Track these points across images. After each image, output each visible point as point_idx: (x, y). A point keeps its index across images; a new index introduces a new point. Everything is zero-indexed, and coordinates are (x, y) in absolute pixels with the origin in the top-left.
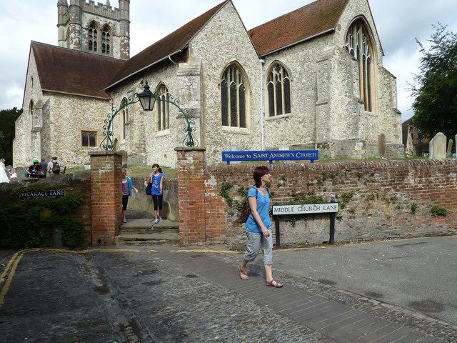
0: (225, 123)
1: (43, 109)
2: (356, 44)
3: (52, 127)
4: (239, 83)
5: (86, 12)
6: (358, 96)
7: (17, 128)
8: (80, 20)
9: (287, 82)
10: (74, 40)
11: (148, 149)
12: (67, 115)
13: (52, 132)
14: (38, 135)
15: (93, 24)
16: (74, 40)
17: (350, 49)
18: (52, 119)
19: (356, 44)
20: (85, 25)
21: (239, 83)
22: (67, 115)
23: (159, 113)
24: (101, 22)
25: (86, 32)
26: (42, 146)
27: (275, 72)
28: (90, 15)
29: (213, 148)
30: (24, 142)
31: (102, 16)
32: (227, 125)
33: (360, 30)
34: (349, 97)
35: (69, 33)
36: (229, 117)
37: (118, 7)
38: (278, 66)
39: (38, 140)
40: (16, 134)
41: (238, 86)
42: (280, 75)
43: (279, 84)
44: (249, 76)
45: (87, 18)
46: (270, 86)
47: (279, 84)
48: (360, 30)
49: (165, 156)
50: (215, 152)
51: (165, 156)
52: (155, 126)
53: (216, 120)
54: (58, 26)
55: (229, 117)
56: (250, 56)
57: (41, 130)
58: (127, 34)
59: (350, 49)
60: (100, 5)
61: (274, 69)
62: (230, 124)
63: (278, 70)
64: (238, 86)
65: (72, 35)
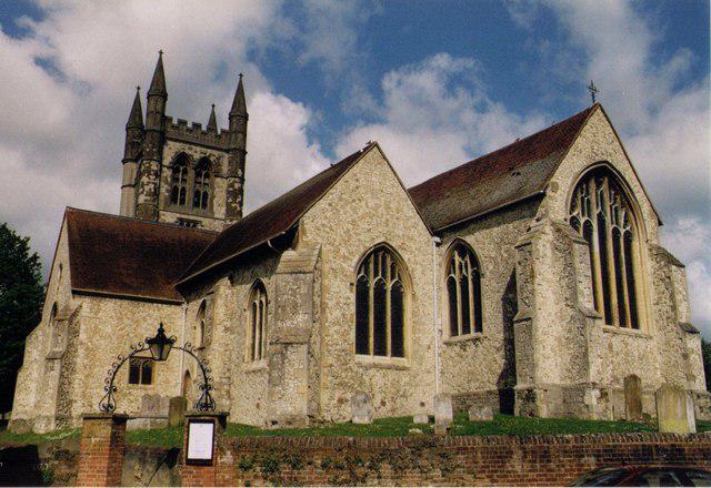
0: (362, 348)
1: (71, 321)
2: (595, 211)
3: (81, 351)
4: (392, 278)
5: (171, 139)
6: (590, 306)
7: (28, 349)
8: (160, 152)
9: (477, 276)
10: (146, 188)
11: (234, 393)
12: (109, 330)
13: (80, 359)
14: (57, 365)
15: (181, 159)
16: (146, 188)
17: (582, 221)
18: (83, 336)
19: (595, 211)
20: (167, 161)
21: (392, 278)
22: (109, 330)
23: (254, 331)
24: (196, 153)
25: (167, 173)
26: (61, 384)
27: (457, 259)
28: (178, 144)
29: (337, 395)
30: (35, 375)
31: (196, 145)
32: (367, 353)
33: (605, 186)
34: (572, 307)
35: (140, 175)
36: (371, 340)
37: (227, 128)
38: (464, 249)
39: (56, 373)
40: (26, 359)
41: (389, 286)
42: (466, 263)
43: (464, 280)
44: (411, 266)
45: (171, 150)
46: (451, 283)
47: (464, 280)
48: (605, 186)
49: (258, 406)
50: (341, 401)
51: (258, 406)
52: (247, 353)
53: (345, 346)
54: (124, 162)
55: (371, 340)
56: (413, 232)
57: (63, 357)
58: (240, 172)
59: (582, 221)
60: (197, 126)
61: (456, 253)
62: (372, 351)
63: (462, 255)
64: (389, 286)
65: (145, 179)
